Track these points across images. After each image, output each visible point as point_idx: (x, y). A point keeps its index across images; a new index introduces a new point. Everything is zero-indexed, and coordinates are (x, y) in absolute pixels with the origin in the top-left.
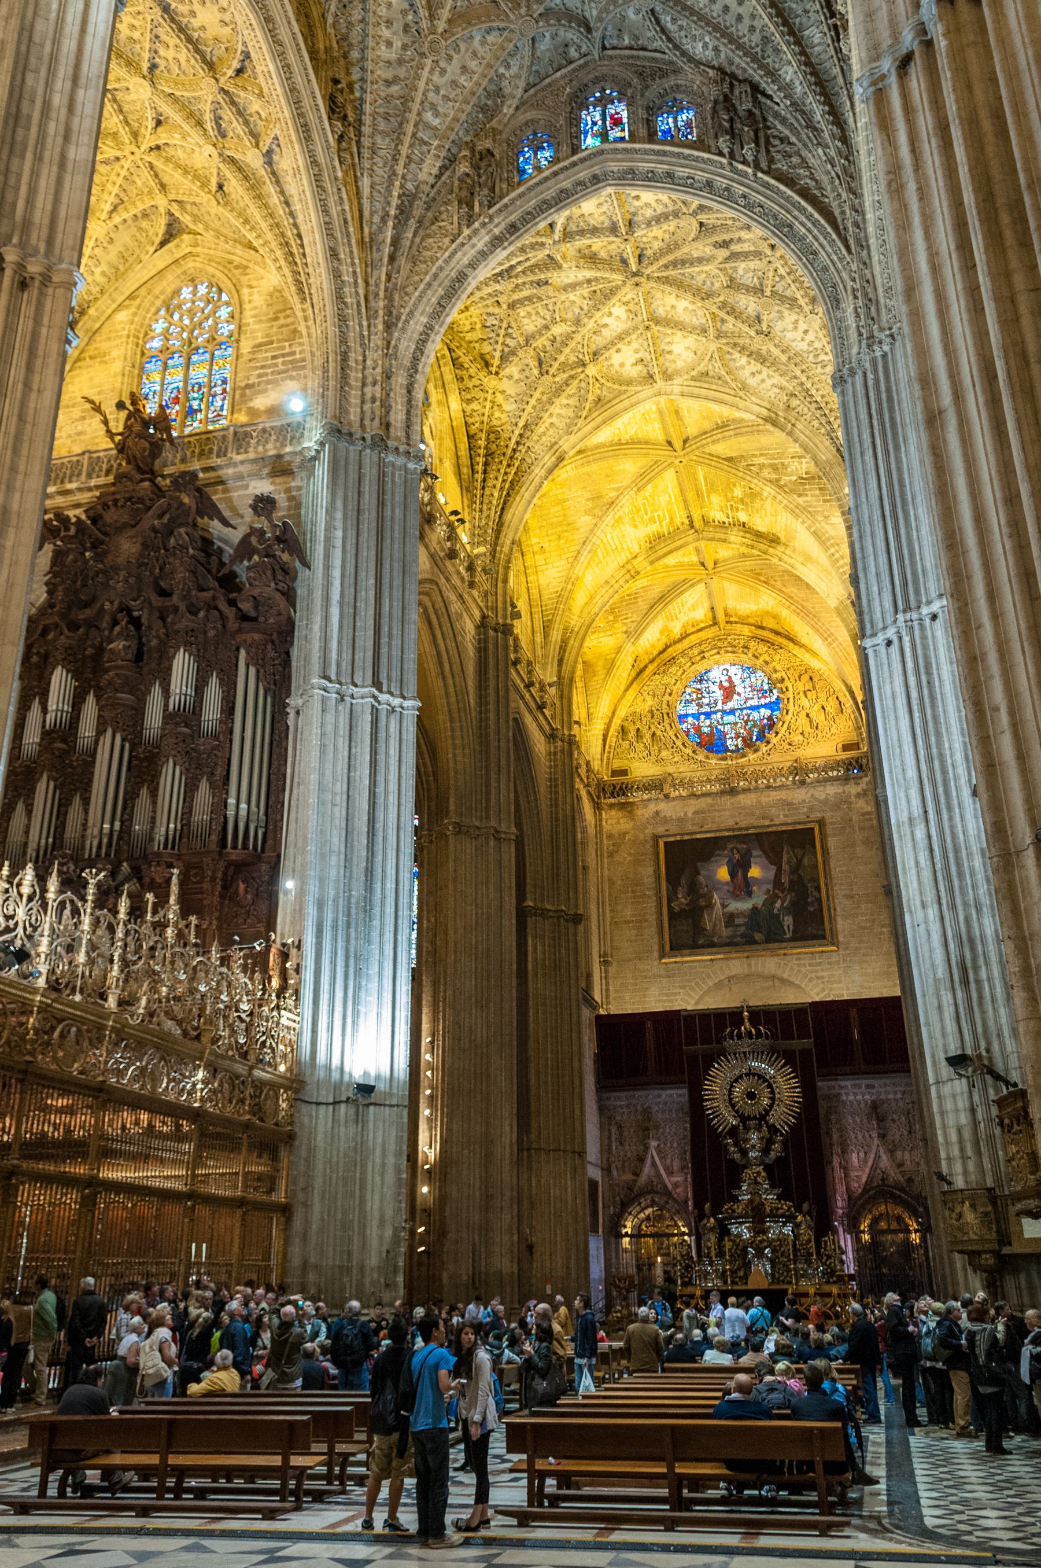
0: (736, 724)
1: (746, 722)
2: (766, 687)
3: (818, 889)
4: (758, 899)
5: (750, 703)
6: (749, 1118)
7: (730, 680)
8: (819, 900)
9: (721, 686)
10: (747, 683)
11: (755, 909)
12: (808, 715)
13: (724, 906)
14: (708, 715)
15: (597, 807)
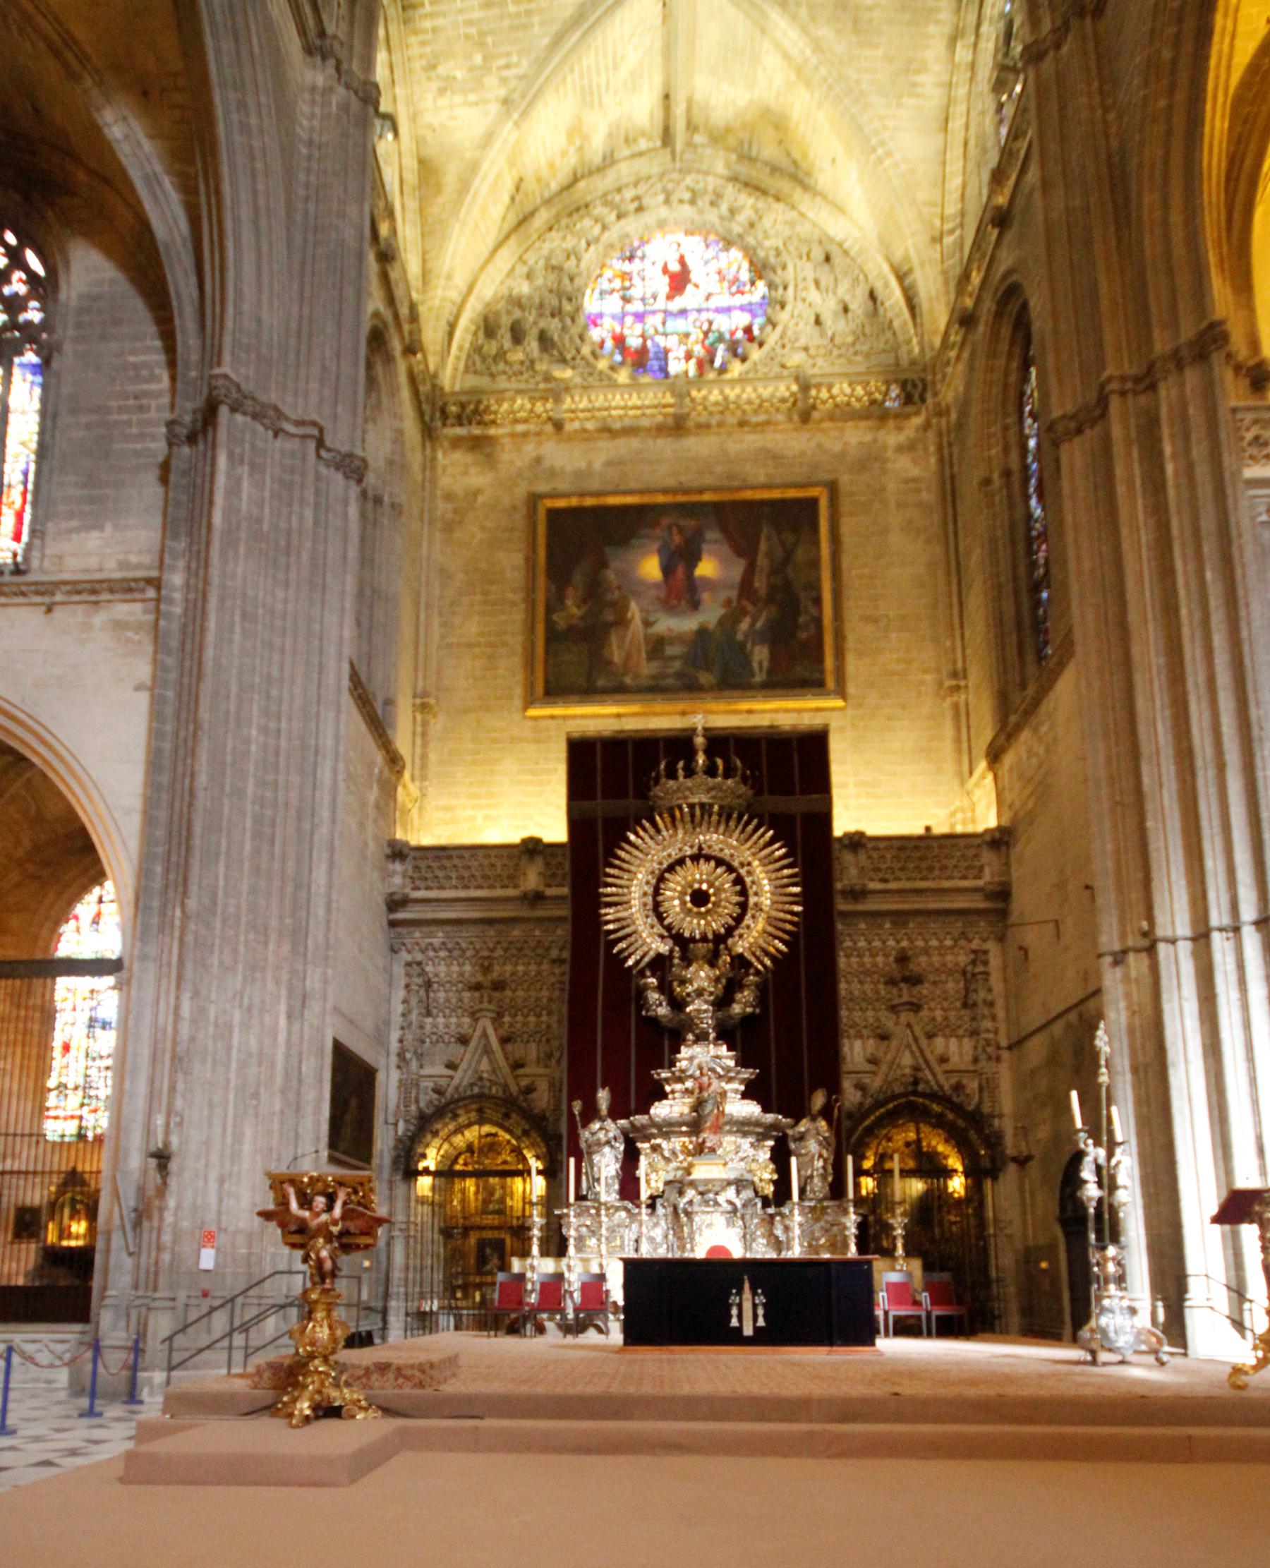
0: (687, 335)
1: (706, 334)
2: (745, 276)
3: (818, 601)
4: (710, 614)
5: (713, 303)
6: (692, 939)
7: (682, 261)
8: (818, 621)
9: (665, 270)
10: (714, 266)
11: (702, 632)
12: (818, 322)
13: (647, 624)
14: (640, 317)
15: (428, 433)
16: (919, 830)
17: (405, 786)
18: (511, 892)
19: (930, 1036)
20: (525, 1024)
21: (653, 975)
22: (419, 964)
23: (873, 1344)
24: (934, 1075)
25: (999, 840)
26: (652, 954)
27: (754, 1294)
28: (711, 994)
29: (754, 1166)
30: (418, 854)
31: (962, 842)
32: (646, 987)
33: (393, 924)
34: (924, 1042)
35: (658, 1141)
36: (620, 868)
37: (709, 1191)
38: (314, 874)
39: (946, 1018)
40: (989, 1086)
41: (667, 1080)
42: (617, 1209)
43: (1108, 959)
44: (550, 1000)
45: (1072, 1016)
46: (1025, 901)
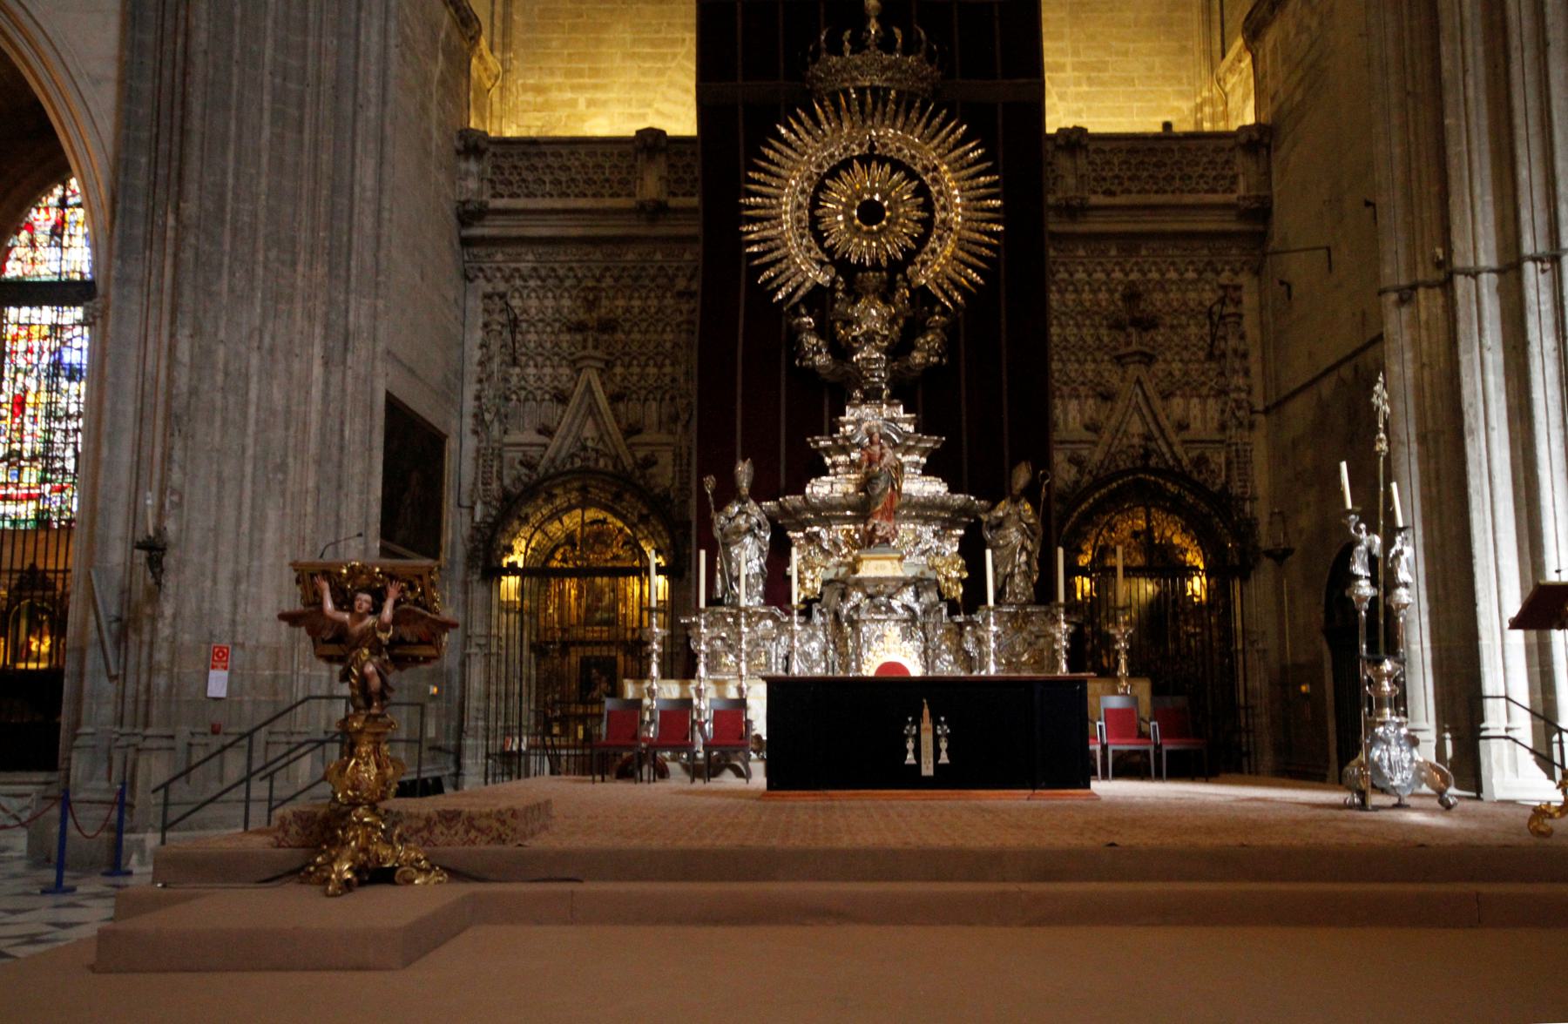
6: (861, 266)
16: (1153, 125)
17: (481, 57)
18: (622, 202)
19: (1166, 396)
20: (642, 377)
21: (809, 314)
22: (502, 296)
23: (1088, 787)
24: (1170, 446)
25: (1257, 141)
26: (808, 284)
27: (936, 722)
28: (885, 338)
29: (938, 561)
30: (499, 150)
31: (1211, 145)
32: (800, 329)
33: (466, 242)
34: (1158, 404)
35: (816, 529)
36: (768, 172)
37: (880, 593)
38: (358, 172)
39: (1186, 373)
40: (1240, 461)
41: (827, 450)
42: (762, 617)
43: (1393, 297)
44: (675, 345)
45: (1346, 371)
46: (1289, 223)
